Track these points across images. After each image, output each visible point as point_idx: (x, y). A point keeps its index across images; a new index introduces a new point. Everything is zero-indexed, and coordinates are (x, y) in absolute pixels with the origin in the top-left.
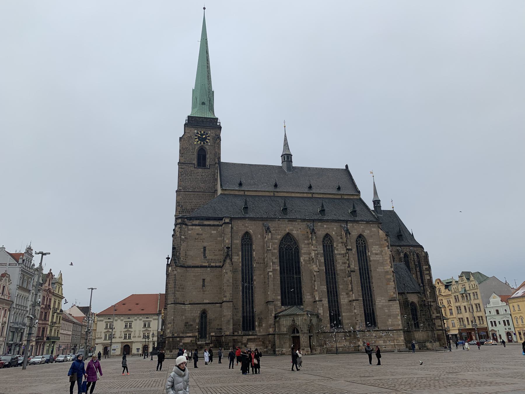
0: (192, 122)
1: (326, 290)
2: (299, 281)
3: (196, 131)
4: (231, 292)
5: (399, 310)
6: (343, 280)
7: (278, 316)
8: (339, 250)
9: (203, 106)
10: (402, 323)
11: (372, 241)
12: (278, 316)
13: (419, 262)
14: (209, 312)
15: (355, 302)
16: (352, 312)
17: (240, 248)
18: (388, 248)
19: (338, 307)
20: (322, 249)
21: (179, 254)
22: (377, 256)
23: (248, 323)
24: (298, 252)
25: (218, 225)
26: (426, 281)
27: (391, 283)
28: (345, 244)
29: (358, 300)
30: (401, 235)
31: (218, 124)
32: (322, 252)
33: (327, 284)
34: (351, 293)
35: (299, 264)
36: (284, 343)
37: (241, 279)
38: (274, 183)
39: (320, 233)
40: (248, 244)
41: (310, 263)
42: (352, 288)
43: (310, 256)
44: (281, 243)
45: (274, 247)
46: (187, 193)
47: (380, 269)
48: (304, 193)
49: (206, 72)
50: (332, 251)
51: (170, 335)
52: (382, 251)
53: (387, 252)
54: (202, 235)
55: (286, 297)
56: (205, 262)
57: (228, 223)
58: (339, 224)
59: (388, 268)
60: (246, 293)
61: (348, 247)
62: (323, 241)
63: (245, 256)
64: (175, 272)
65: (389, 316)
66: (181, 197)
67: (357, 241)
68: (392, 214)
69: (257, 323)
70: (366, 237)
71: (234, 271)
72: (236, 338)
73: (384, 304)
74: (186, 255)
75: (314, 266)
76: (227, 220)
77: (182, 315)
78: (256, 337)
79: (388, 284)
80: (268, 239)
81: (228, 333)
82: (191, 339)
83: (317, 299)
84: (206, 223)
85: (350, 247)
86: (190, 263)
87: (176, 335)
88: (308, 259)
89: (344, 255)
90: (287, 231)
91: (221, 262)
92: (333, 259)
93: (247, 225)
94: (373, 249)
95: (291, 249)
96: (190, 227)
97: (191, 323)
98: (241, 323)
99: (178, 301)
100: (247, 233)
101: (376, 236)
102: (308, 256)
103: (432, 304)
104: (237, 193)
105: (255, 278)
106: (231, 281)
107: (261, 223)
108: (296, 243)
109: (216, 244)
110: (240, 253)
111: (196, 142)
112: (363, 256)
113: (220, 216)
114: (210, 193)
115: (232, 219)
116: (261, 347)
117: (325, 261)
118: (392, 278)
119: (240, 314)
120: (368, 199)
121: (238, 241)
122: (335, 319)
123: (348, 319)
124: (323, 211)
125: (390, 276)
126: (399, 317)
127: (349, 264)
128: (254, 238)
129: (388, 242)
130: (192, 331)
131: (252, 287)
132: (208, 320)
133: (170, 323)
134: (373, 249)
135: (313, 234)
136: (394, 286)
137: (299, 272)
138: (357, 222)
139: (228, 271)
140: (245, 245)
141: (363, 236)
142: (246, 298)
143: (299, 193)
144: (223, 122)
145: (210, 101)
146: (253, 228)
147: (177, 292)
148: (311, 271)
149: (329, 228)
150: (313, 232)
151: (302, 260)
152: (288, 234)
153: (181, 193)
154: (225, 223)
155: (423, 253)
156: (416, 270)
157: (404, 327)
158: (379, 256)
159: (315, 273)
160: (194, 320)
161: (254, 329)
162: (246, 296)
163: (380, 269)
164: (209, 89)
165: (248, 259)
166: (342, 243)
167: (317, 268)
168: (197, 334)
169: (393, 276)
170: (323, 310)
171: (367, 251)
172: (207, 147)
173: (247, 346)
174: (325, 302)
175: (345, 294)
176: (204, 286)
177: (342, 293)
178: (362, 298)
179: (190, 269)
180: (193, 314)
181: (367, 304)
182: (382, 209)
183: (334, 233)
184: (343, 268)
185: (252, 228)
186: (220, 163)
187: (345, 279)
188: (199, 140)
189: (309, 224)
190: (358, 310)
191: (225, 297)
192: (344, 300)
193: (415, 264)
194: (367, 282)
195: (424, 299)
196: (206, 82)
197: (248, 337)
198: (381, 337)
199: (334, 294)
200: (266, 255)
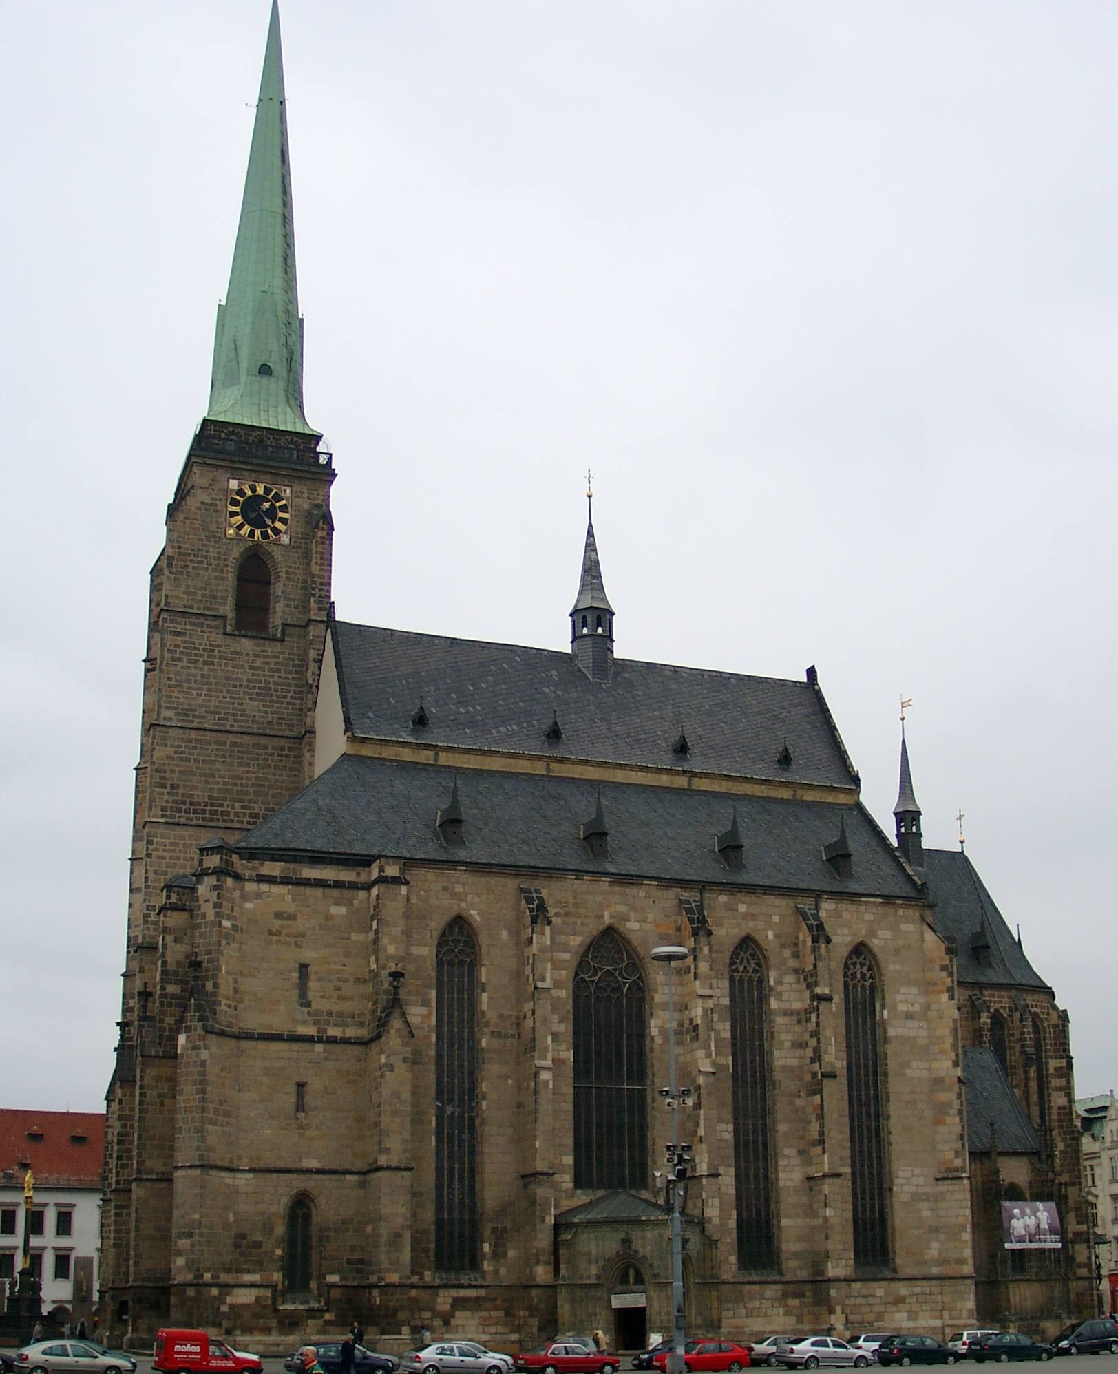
0: (215, 445)
1: (729, 1136)
2: (639, 1104)
3: (234, 484)
4: (407, 1135)
5: (968, 1212)
6: (792, 1103)
7: (569, 1226)
8: (786, 996)
9: (265, 380)
10: (974, 1258)
11: (898, 967)
12: (569, 1226)
13: (1038, 1044)
14: (321, 1200)
15: (829, 1181)
16: (813, 1217)
17: (434, 974)
18: (952, 998)
19: (767, 1199)
20: (727, 992)
21: (216, 985)
22: (910, 1023)
23: (455, 1242)
24: (642, 1000)
25: (353, 886)
26: (1055, 1111)
27: (948, 1120)
28: (810, 979)
29: (838, 1175)
30: (988, 947)
31: (323, 460)
32: (726, 1001)
33: (735, 1118)
34: (819, 1149)
35: (641, 1045)
36: (590, 1315)
37: (433, 1092)
38: (546, 725)
40: (461, 963)
41: (680, 1043)
42: (821, 1133)
43: (685, 1013)
44: (582, 966)
45: (555, 979)
46: (193, 735)
47: (917, 1070)
48: (658, 770)
49: (279, 240)
50: (763, 999)
51: (190, 1277)
52: (928, 1007)
53: (947, 1008)
54: (293, 917)
55: (589, 1158)
56: (304, 1023)
57: (396, 881)
58: (791, 902)
59: (945, 1067)
60: (451, 1141)
61: (818, 990)
62: (732, 964)
63: (450, 1006)
64: (204, 1055)
65: (934, 1230)
66: (169, 751)
67: (846, 966)
68: (957, 865)
69: (486, 1247)
70: (879, 955)
71: (414, 1060)
72: (414, 1292)
73: (921, 1190)
74: (236, 991)
75: (700, 1054)
76: (392, 870)
78: (482, 1292)
79: (939, 1122)
80: (542, 949)
81: (394, 1278)
82: (255, 1292)
83: (703, 1168)
84: (309, 872)
85: (827, 991)
86: (252, 1021)
88: (674, 1025)
89: (802, 1017)
90: (607, 920)
91: (362, 1024)
92: (761, 1030)
93: (459, 889)
94: (898, 997)
95: (620, 989)
96: (251, 887)
97: (258, 1237)
98: (433, 1246)
99: (214, 1158)
100: (459, 923)
101: (910, 950)
102: (676, 1015)
103: (1070, 1189)
104: (407, 755)
105: (484, 1087)
106: (407, 1096)
107: (512, 884)
108: (636, 965)
109: (347, 954)
110: (433, 994)
111: (235, 527)
112: (865, 1020)
113: (359, 849)
114: (283, 742)
115: (410, 863)
116: (500, 1329)
117: (734, 1037)
118: (956, 1104)
119: (429, 1215)
120: (879, 800)
121: (426, 951)
122: (758, 1240)
123: (800, 1239)
124: (730, 849)
125: (950, 1096)
126: (967, 1236)
127: (817, 1050)
128: (484, 940)
129: (951, 975)
130: (260, 1266)
131: (472, 1119)
132: (314, 1230)
133: (189, 1235)
134: (898, 997)
135: (703, 939)
136: (957, 1129)
137: (639, 1067)
138: (852, 897)
139: (397, 1061)
140: (451, 963)
141: (870, 950)
142: (451, 1158)
143: (640, 769)
144: (337, 445)
145: (290, 360)
146: (484, 902)
147: (210, 1128)
148: (686, 1073)
150: (700, 927)
151: (654, 1031)
152: (610, 931)
153: (172, 733)
154: (382, 880)
155: (1054, 1015)
156: (1026, 1072)
157: (977, 1268)
158: (915, 1023)
159: (701, 1080)
160: (268, 1228)
161: (474, 1263)
162: (451, 1151)
163: (917, 1070)
164: (287, 312)
165: (461, 1016)
166: (796, 971)
167: (707, 1061)
168: (277, 1277)
169: (959, 1096)
170: (718, 1205)
171: (878, 1005)
172: (278, 554)
173: (453, 1322)
174: (728, 1180)
175: (794, 1152)
176: (300, 1107)
177: (786, 1151)
178: (847, 1170)
179: (253, 1043)
180: (261, 1207)
181: (863, 1190)
182: (926, 844)
183: (770, 935)
184: (795, 1062)
186: (330, 621)
187: (799, 1102)
188: (247, 520)
189: (686, 895)
190: (837, 1211)
191: (387, 1151)
192: (789, 1174)
193: (1023, 1053)
194: (868, 1115)
195: (1051, 1175)
196: (278, 282)
197: (454, 1293)
198: (900, 1300)
199: (756, 1151)
200: (528, 1007)
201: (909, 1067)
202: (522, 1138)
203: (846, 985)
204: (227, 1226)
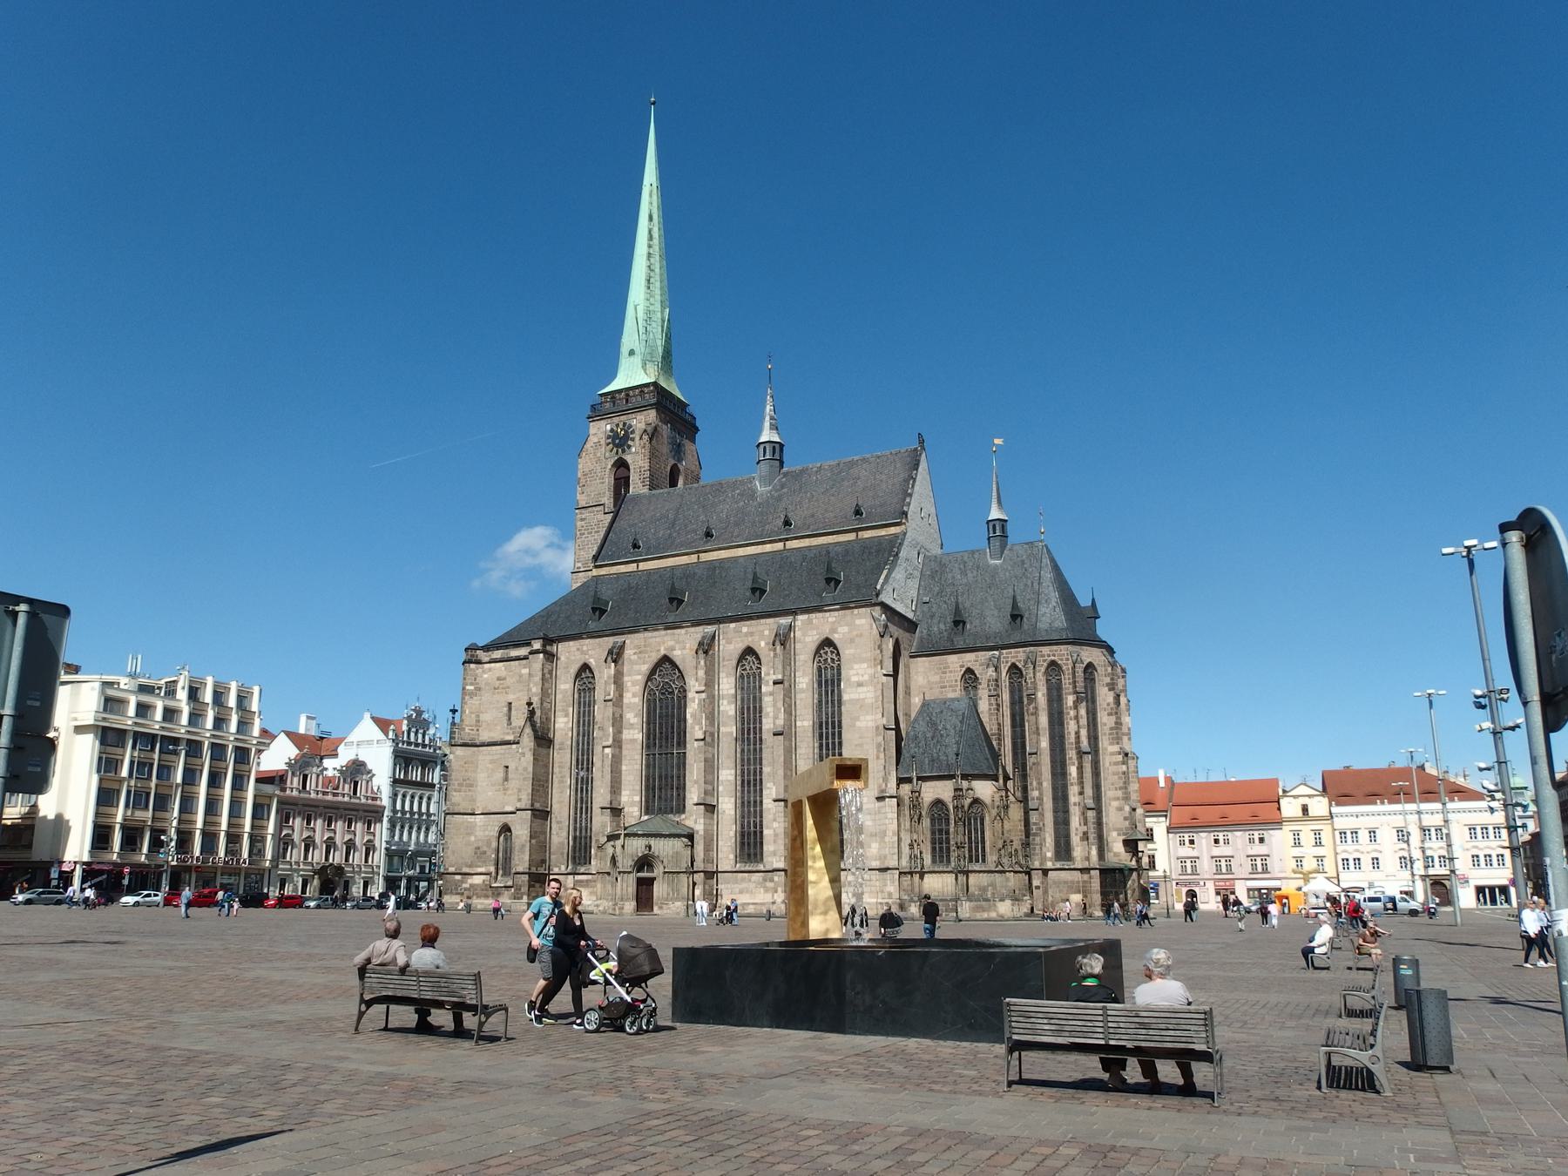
22: (860, 689)
39: (731, 647)
77: (469, 834)
81: (520, 869)
84: (514, 653)
86: (485, 736)
87: (452, 870)
90: (663, 652)
100: (585, 667)
121: (565, 685)
130: (485, 863)
149: (752, 634)
152: (666, 659)
160: (489, 844)
168: (492, 869)
172: (628, 458)
176: (506, 779)
185: (592, 651)
201: (857, 719)
202: (616, 788)
203: (819, 669)
204: (468, 844)
